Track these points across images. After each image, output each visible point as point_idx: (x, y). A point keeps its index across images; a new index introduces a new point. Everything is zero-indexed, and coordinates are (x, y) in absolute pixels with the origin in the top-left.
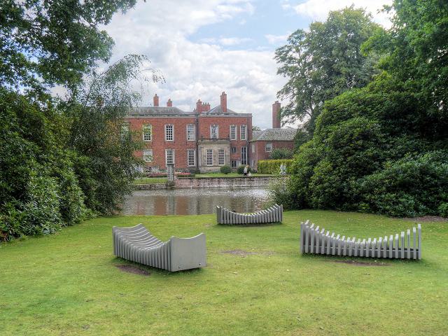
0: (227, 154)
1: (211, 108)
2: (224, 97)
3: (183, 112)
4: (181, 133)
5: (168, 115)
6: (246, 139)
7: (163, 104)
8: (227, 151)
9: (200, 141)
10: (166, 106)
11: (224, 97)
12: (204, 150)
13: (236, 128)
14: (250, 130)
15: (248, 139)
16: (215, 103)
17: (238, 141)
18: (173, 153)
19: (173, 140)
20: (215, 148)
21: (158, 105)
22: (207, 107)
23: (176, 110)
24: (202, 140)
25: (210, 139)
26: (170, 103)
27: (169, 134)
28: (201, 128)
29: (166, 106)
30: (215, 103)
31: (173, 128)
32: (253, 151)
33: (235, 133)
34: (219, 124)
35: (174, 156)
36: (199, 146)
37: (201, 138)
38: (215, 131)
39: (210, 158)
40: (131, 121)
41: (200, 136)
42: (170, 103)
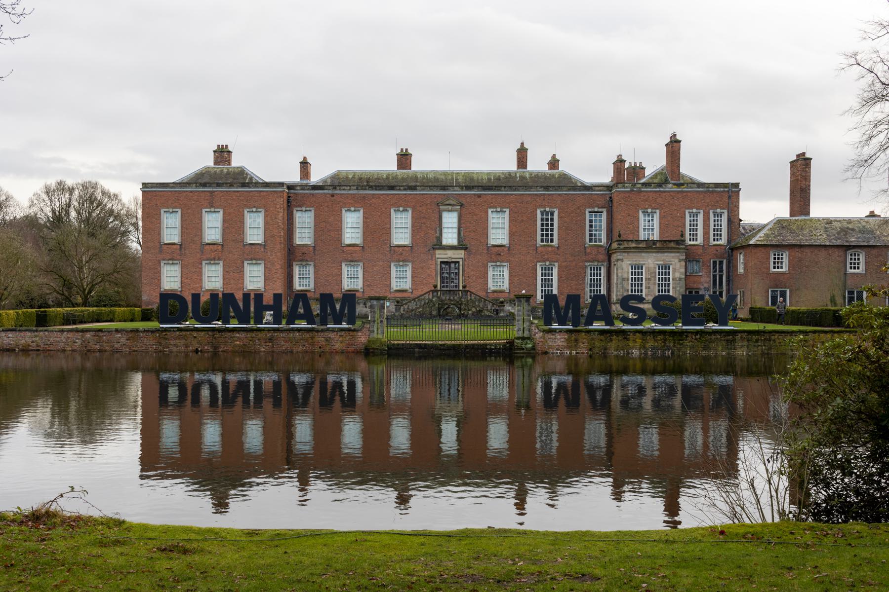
0: (677, 275)
1: (649, 172)
2: (674, 146)
3: (577, 180)
4: (573, 225)
6: (723, 241)
7: (537, 164)
9: (615, 245)
10: (544, 168)
11: (674, 146)
12: (624, 266)
13: (700, 218)
14: (734, 221)
15: (729, 241)
16: (654, 163)
17: (706, 245)
18: (555, 272)
19: (555, 243)
20: (651, 261)
21: (525, 167)
22: (637, 171)
23: (565, 177)
24: (620, 241)
25: (638, 241)
26: (554, 163)
27: (547, 229)
28: (618, 217)
29: (544, 168)
30: (654, 163)
32: (741, 270)
33: (702, 229)
34: (660, 207)
36: (614, 257)
37: (622, 241)
40: (463, 201)
41: (616, 237)
42: (554, 163)
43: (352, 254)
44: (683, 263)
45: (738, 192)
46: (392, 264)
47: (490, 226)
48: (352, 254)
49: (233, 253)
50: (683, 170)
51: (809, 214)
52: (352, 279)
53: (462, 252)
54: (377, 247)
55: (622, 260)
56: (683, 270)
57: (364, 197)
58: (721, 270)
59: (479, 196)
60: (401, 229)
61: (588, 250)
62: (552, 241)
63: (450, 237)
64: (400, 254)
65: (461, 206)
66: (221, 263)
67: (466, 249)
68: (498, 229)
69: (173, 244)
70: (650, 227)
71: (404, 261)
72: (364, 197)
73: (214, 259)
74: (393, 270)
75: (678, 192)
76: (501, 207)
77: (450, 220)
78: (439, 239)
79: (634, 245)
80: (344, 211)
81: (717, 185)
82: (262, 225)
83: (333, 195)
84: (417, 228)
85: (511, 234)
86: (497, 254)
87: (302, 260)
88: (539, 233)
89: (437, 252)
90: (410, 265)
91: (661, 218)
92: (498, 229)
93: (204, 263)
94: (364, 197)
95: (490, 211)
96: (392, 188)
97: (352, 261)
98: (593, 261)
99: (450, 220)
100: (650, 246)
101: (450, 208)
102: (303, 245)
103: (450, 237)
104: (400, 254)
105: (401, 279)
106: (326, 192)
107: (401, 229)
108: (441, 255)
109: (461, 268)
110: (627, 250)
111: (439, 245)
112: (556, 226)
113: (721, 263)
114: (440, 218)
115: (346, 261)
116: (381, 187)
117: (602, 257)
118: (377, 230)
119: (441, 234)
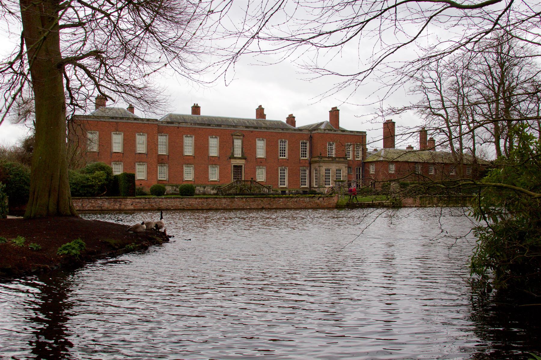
0: (344, 174)
2: (335, 113)
5: (282, 129)
8: (344, 172)
14: (364, 150)
15: (363, 158)
18: (286, 172)
20: (334, 167)
35: (286, 175)
39: (327, 177)
43: (188, 161)
44: (347, 168)
45: (366, 136)
46: (209, 166)
47: (257, 147)
48: (188, 161)
49: (201, 158)
50: (340, 126)
51: (394, 146)
52: (189, 175)
53: (244, 160)
54: (201, 158)
55: (322, 166)
56: (347, 172)
57: (195, 130)
58: (359, 172)
59: (252, 132)
60: (214, 147)
61: (301, 161)
62: (285, 156)
63: (238, 152)
64: (213, 161)
65: (243, 136)
66: (122, 163)
67: (245, 159)
68: (261, 149)
69: (95, 152)
71: (215, 165)
72: (195, 130)
73: (118, 161)
74: (210, 169)
75: (343, 134)
76: (263, 138)
77: (238, 143)
78: (233, 154)
79: (327, 159)
80: (184, 136)
81: (357, 132)
82: (145, 142)
83: (178, 128)
84: (222, 147)
85: (267, 152)
86: (260, 162)
87: (162, 163)
88: (279, 152)
89: (232, 160)
90: (218, 166)
92: (261, 149)
93: (112, 163)
94: (195, 129)
95: (257, 139)
96: (209, 125)
97: (188, 164)
98: (304, 167)
99: (238, 143)
100: (333, 160)
101: (238, 137)
102: (162, 155)
103: (238, 152)
104: (213, 161)
105: (214, 175)
106: (174, 125)
107: (214, 147)
108: (234, 162)
109: (243, 169)
110: (324, 162)
111: (232, 157)
112: (287, 149)
113: (359, 169)
114: (233, 142)
115: (186, 164)
116: (204, 124)
117: (307, 165)
118: (201, 147)
119: (233, 151)
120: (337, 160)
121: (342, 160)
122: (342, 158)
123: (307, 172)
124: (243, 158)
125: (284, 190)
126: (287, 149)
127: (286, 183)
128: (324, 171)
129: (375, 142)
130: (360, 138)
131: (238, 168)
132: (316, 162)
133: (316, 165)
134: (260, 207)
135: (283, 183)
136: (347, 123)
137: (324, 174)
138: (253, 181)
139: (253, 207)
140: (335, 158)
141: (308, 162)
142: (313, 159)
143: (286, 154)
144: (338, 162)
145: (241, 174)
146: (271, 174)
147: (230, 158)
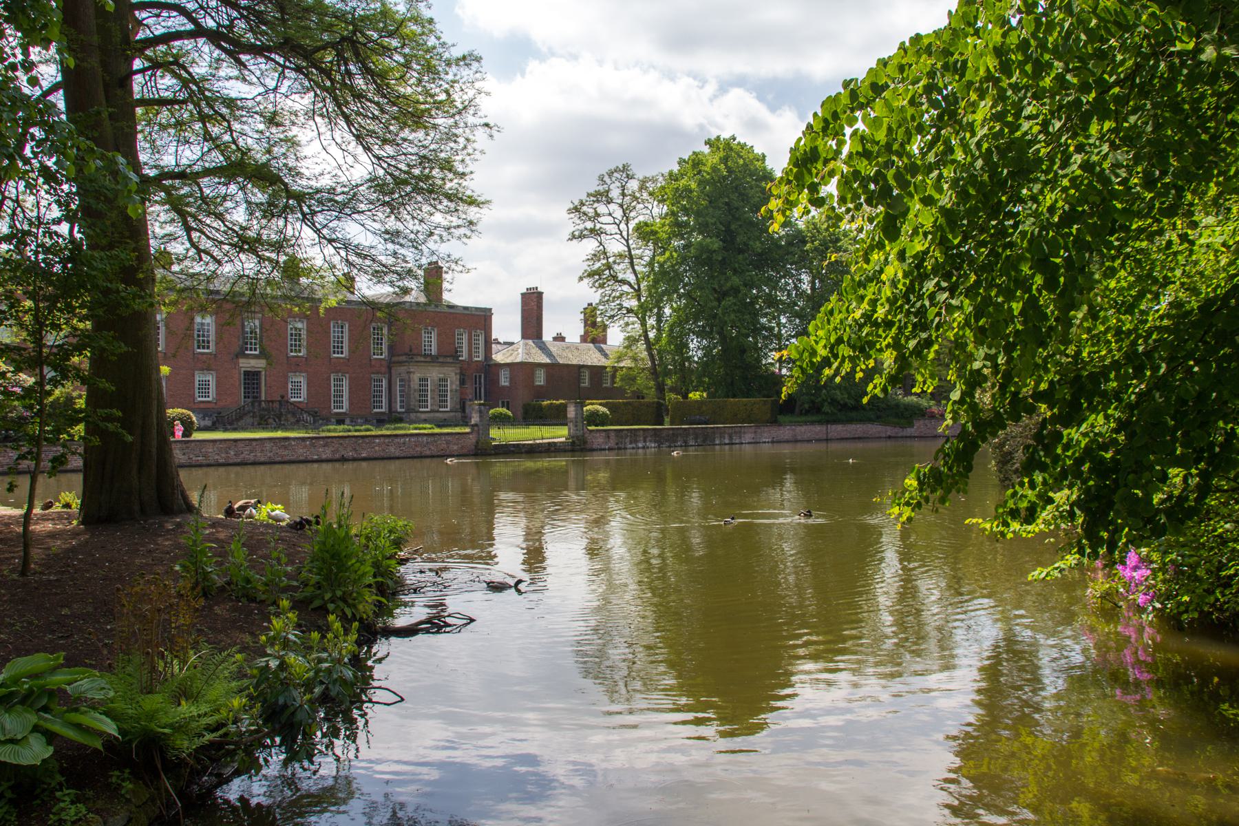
18: (346, 383)
20: (434, 374)
31: (346, 329)
35: (346, 389)
38: (431, 342)
70: (431, 342)
81: (477, 309)
89: (241, 361)
91: (439, 335)
98: (378, 373)
100: (434, 360)
117: (383, 369)
120: (441, 360)
121: (449, 360)
122: (448, 355)
123: (384, 383)
124: (263, 355)
125: (341, 417)
126: (346, 340)
127: (346, 404)
128: (417, 381)
129: (507, 328)
130: (480, 319)
131: (252, 378)
132: (401, 363)
133: (402, 369)
134: (337, 456)
135: (339, 404)
136: (459, 292)
137: (417, 387)
138: (283, 401)
139: (324, 457)
140: (437, 357)
141: (384, 363)
142: (395, 359)
143: (346, 349)
144: (443, 364)
145: (259, 388)
146: (319, 388)
147: (237, 356)
